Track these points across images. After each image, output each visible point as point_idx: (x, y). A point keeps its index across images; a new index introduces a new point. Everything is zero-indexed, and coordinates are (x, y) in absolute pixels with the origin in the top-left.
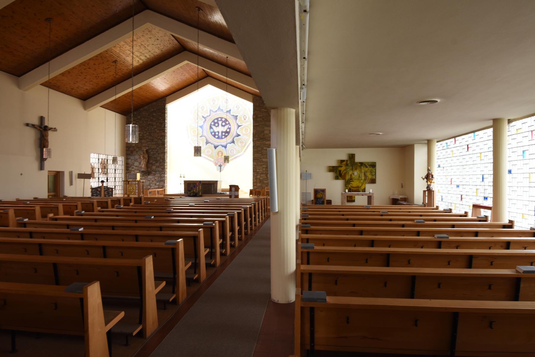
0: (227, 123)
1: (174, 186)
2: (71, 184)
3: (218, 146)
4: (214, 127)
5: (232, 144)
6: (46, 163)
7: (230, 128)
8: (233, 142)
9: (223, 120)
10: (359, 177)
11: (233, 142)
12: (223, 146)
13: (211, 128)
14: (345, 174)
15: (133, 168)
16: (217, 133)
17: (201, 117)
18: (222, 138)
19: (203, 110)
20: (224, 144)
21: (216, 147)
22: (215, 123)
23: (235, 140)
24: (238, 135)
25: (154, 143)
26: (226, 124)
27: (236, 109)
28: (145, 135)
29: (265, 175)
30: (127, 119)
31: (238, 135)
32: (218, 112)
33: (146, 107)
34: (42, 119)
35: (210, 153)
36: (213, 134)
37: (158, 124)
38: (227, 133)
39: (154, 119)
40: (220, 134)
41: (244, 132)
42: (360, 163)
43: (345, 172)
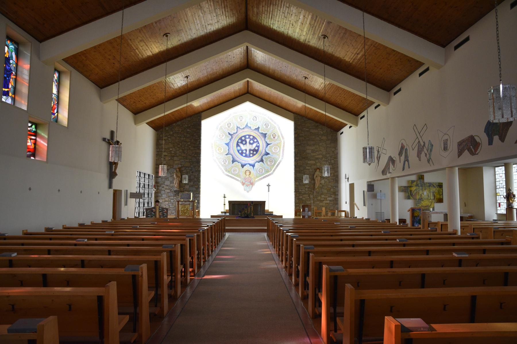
0: (255, 140)
2: (126, 204)
3: (245, 165)
5: (261, 163)
6: (115, 180)
7: (258, 147)
8: (262, 161)
9: (251, 137)
10: (429, 196)
11: (262, 161)
12: (250, 165)
13: (238, 145)
14: (416, 194)
15: (163, 187)
16: (244, 152)
18: (250, 157)
20: (252, 162)
21: (243, 166)
22: (242, 141)
23: (264, 159)
24: (267, 154)
25: (188, 161)
28: (178, 152)
29: (307, 195)
30: (157, 134)
31: (267, 154)
32: (246, 130)
33: (179, 123)
34: (112, 133)
35: (237, 172)
36: (240, 152)
37: (192, 141)
39: (188, 135)
40: (248, 152)
42: (428, 183)
43: (415, 191)
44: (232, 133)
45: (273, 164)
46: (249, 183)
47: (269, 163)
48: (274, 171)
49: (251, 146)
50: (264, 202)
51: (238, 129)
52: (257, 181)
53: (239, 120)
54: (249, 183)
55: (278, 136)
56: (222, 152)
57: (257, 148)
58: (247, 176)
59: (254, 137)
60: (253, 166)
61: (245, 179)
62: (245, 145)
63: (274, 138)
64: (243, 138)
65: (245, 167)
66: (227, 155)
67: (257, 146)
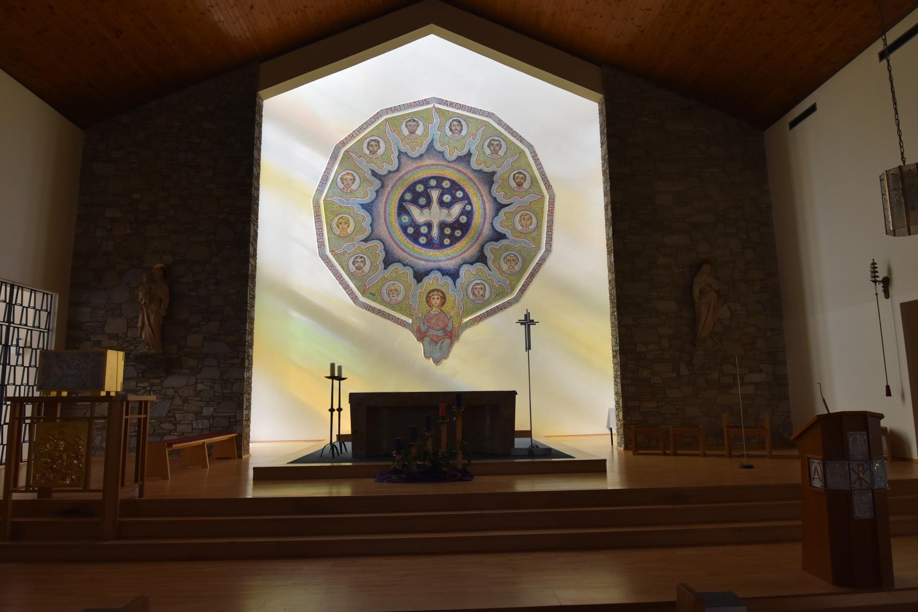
0: (459, 194)
1: (288, 418)
3: (427, 273)
5: (479, 265)
7: (469, 214)
8: (481, 258)
9: (446, 185)
12: (444, 272)
13: (402, 210)
16: (424, 230)
17: (369, 175)
18: (442, 246)
19: (373, 152)
20: (450, 265)
21: (419, 276)
22: (417, 194)
23: (487, 252)
24: (498, 236)
26: (455, 200)
27: (488, 151)
32: (427, 161)
35: (400, 298)
36: (411, 230)
38: (461, 228)
40: (435, 232)
41: (519, 228)
44: (382, 172)
45: (517, 268)
46: (439, 336)
47: (505, 267)
48: (523, 291)
49: (445, 211)
50: (514, 393)
51: (404, 159)
53: (406, 132)
54: (440, 333)
55: (534, 180)
56: (350, 230)
57: (464, 219)
58: (435, 311)
59: (453, 182)
60: (454, 275)
61: (427, 319)
62: (426, 211)
63: (520, 185)
64: (420, 188)
65: (426, 280)
66: (365, 241)
67: (464, 212)
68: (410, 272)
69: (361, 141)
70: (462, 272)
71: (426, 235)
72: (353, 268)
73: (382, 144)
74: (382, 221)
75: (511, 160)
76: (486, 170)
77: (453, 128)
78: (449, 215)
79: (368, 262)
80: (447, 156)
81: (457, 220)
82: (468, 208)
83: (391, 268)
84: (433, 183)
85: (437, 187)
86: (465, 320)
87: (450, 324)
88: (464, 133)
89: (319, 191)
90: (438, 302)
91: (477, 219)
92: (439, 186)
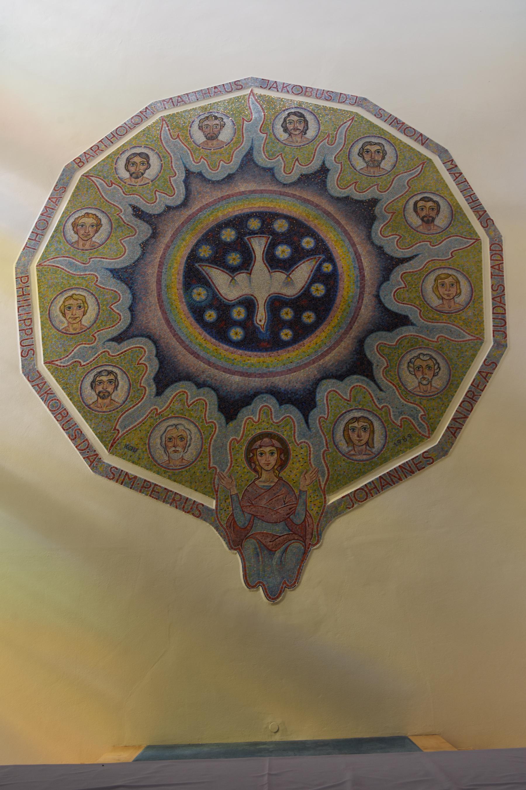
0: (308, 243)
3: (247, 399)
4: (219, 278)
5: (356, 381)
7: (331, 280)
8: (359, 365)
12: (283, 397)
13: (193, 276)
16: (239, 313)
17: (127, 216)
18: (276, 344)
20: (295, 380)
21: (231, 406)
22: (227, 246)
23: (372, 352)
24: (392, 321)
26: (299, 255)
27: (360, 164)
35: (190, 454)
36: (211, 316)
40: (261, 317)
41: (435, 302)
45: (438, 383)
46: (275, 537)
47: (412, 382)
49: (280, 276)
51: (196, 185)
52: (338, 510)
53: (199, 137)
54: (279, 529)
55: (455, 212)
56: (87, 321)
57: (319, 290)
60: (304, 401)
62: (241, 277)
63: (428, 221)
65: (245, 415)
66: (119, 339)
67: (318, 276)
68: (210, 399)
69: (114, 158)
70: (321, 396)
71: (241, 324)
72: (90, 396)
73: (154, 160)
74: (153, 299)
75: (406, 177)
76: (357, 196)
77: (290, 127)
78: (289, 283)
79: (123, 383)
80: (281, 175)
81: (306, 292)
82: (327, 268)
83: (170, 392)
84: (254, 224)
85: (261, 232)
86: (333, 499)
87: (300, 509)
88: (311, 133)
89: (30, 248)
90: (273, 460)
91: (347, 287)
92: (266, 229)
